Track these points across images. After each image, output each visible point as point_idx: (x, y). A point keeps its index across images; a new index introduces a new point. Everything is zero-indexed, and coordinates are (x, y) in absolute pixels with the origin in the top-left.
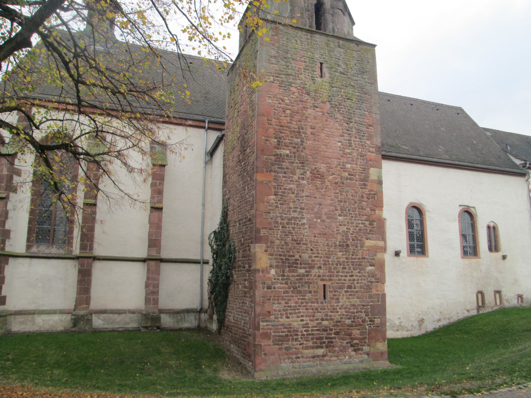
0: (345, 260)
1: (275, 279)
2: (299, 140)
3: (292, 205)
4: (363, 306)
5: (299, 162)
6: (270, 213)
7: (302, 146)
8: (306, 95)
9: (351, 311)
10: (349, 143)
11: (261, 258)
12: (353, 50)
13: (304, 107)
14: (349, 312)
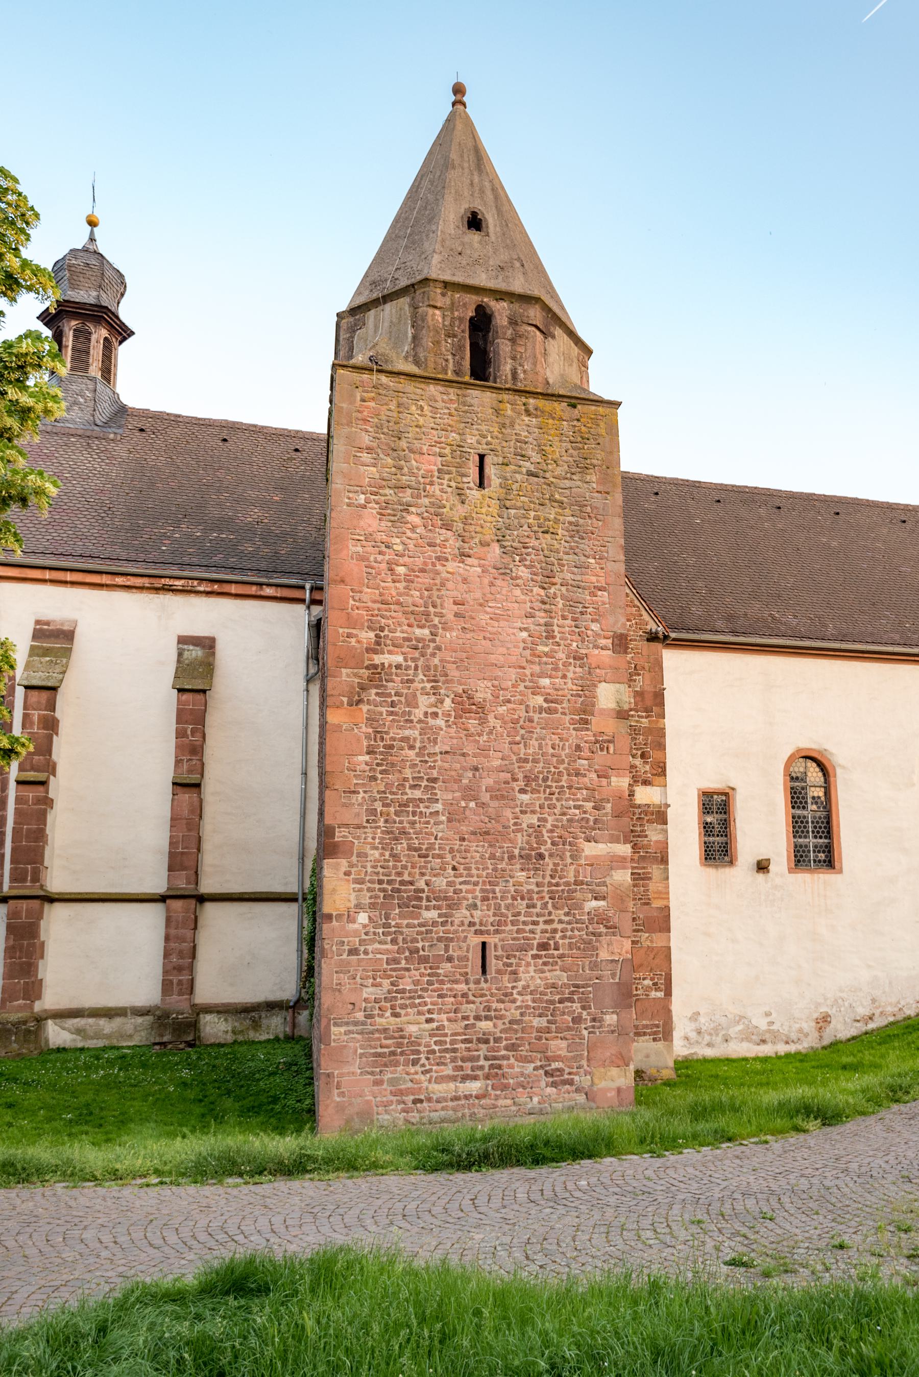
0: (533, 887)
1: (366, 934)
2: (426, 632)
3: (408, 773)
4: (577, 986)
5: (425, 679)
6: (359, 793)
7: (432, 645)
8: (444, 531)
9: (546, 998)
10: (548, 632)
11: (334, 890)
12: (561, 419)
13: (438, 558)
14: (541, 1001)
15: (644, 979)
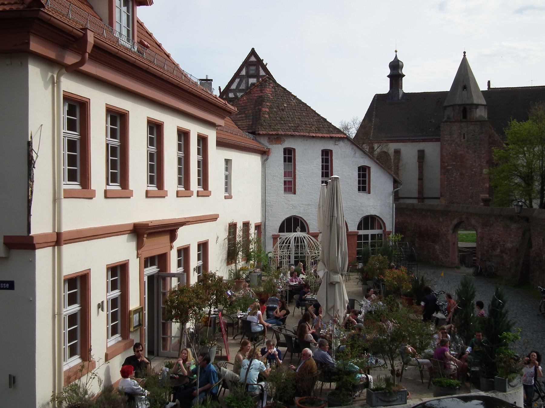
3: (452, 185)
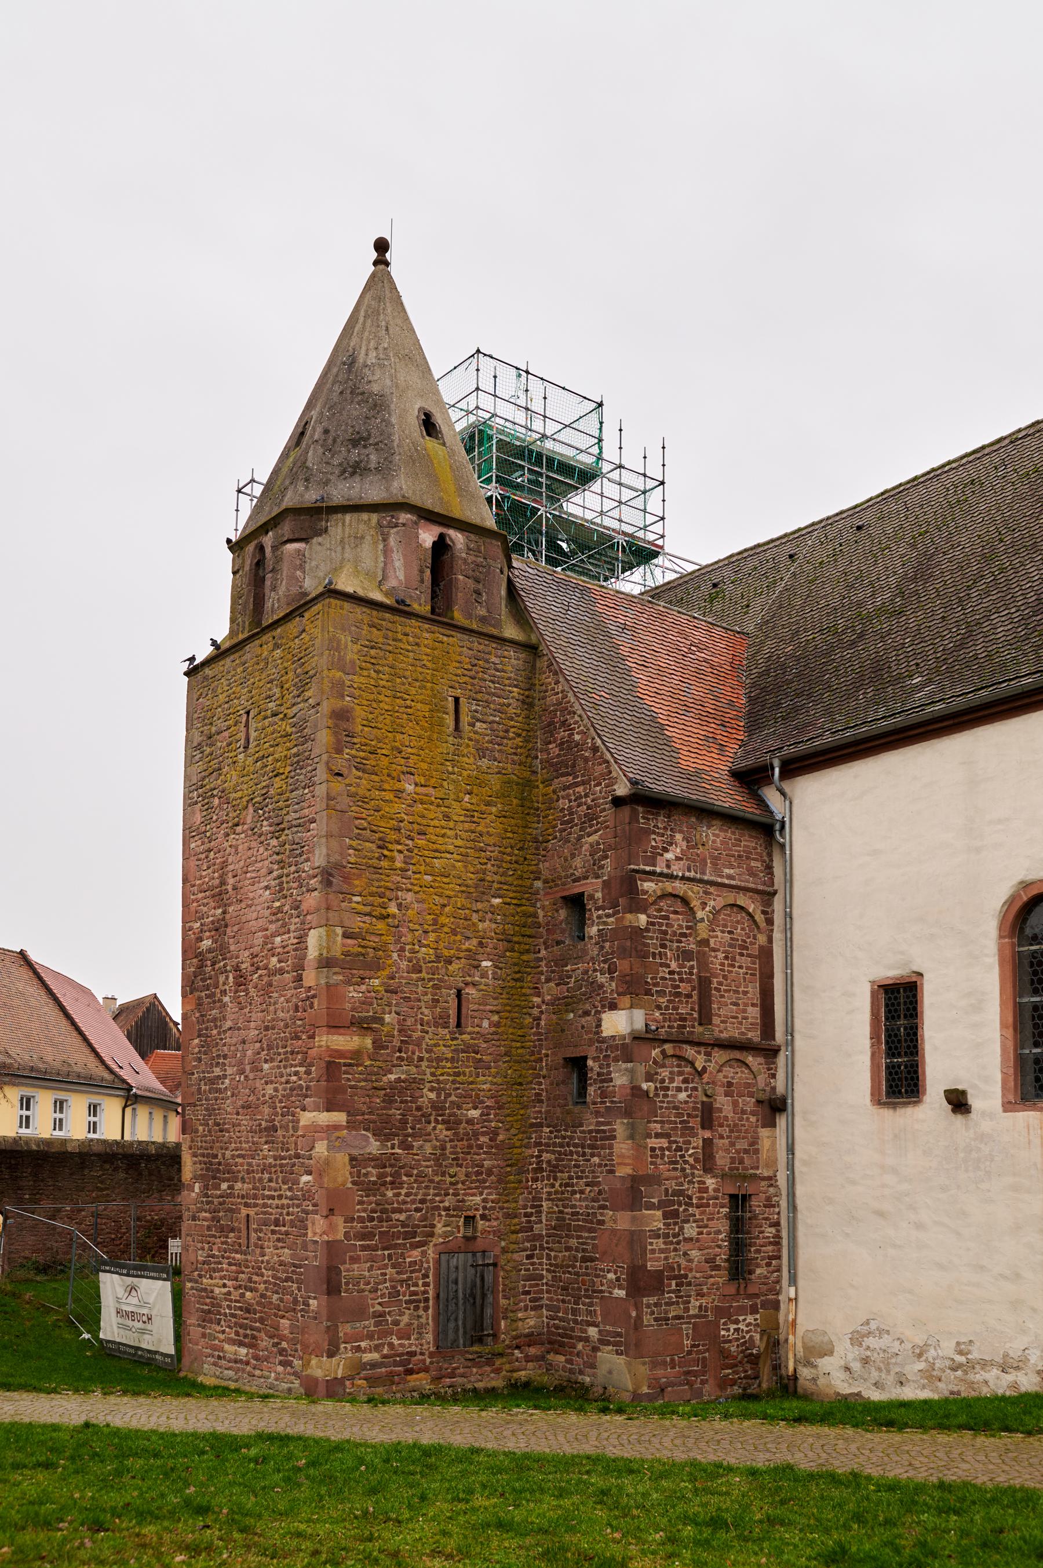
15: (609, 1271)
